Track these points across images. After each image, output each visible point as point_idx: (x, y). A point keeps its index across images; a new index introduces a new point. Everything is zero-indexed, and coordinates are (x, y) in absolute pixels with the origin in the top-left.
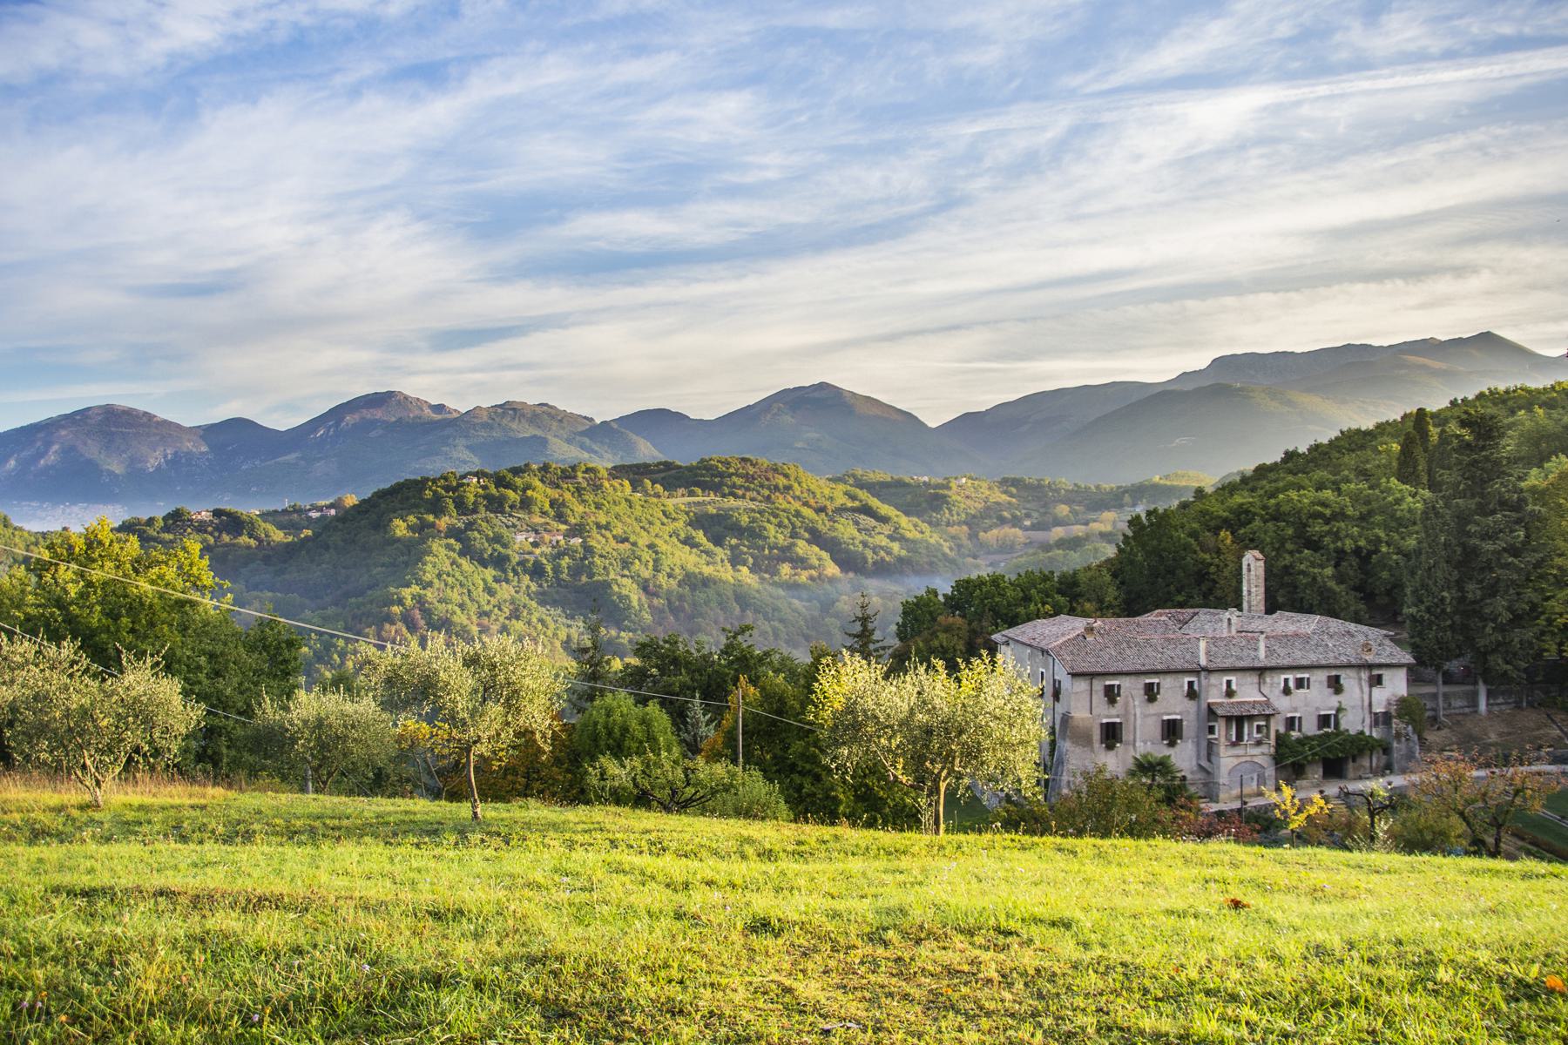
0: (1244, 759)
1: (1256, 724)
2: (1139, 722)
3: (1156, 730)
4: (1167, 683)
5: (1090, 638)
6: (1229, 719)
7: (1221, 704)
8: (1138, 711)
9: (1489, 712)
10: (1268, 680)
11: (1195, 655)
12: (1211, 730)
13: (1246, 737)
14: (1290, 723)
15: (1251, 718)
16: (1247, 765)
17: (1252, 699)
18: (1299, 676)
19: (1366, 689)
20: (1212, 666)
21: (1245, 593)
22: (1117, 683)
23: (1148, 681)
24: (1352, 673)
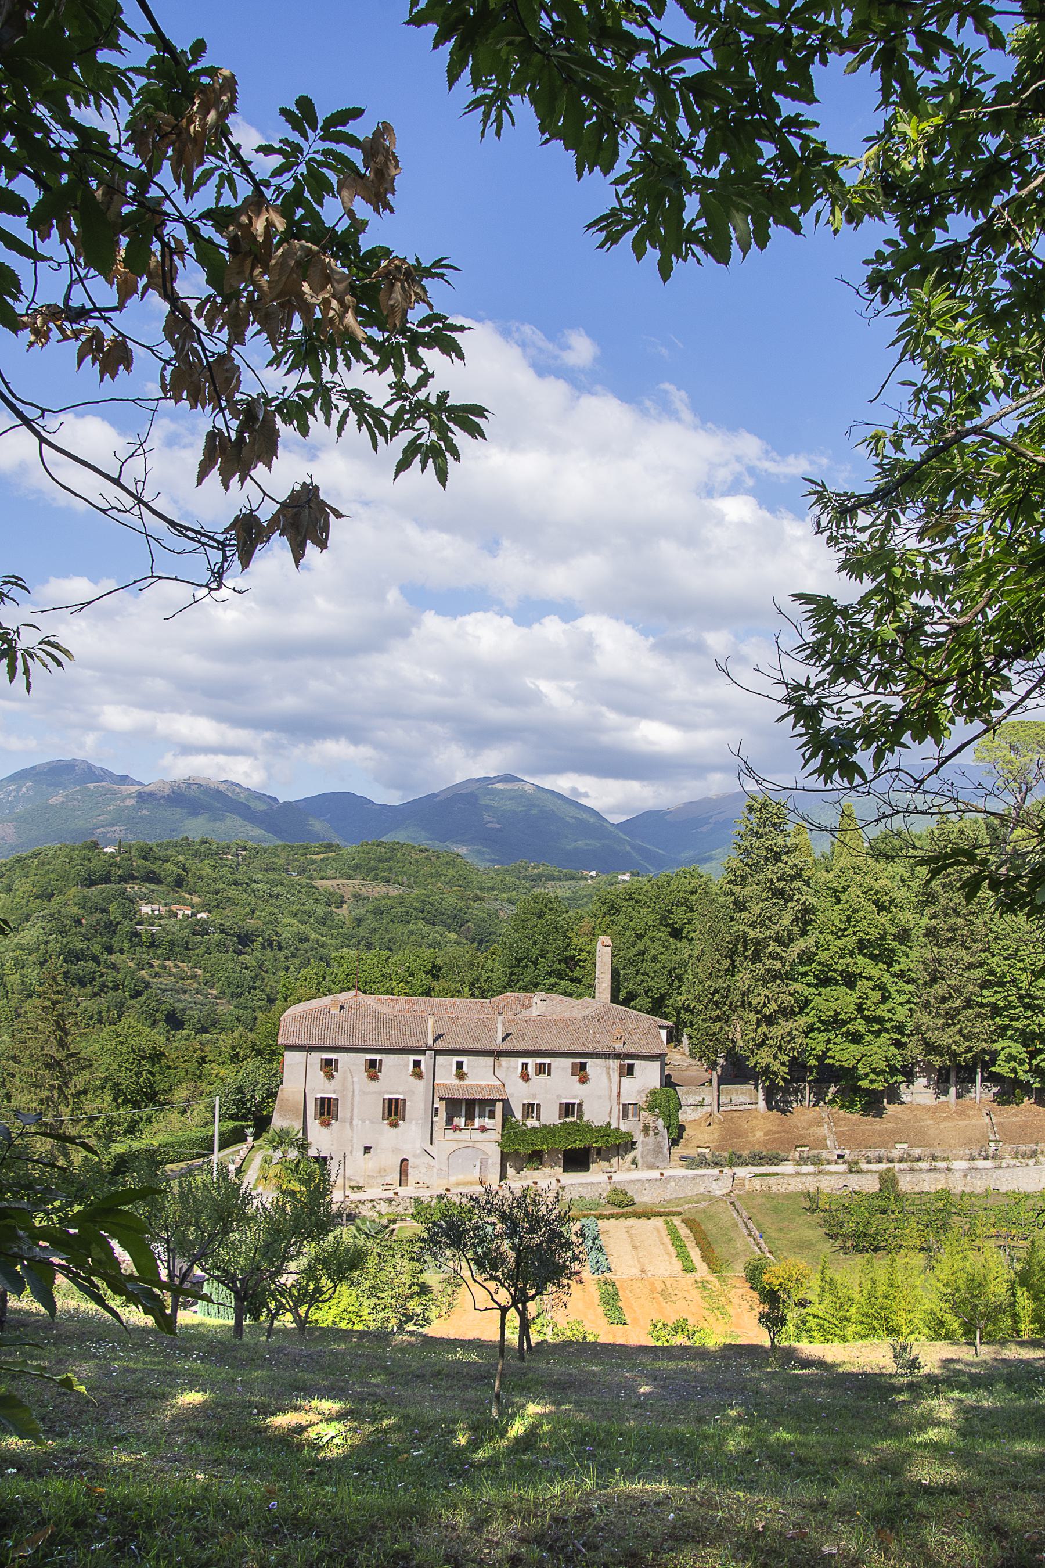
2: (357, 1099)
8: (357, 1087)
16: (470, 1150)
17: (485, 1083)
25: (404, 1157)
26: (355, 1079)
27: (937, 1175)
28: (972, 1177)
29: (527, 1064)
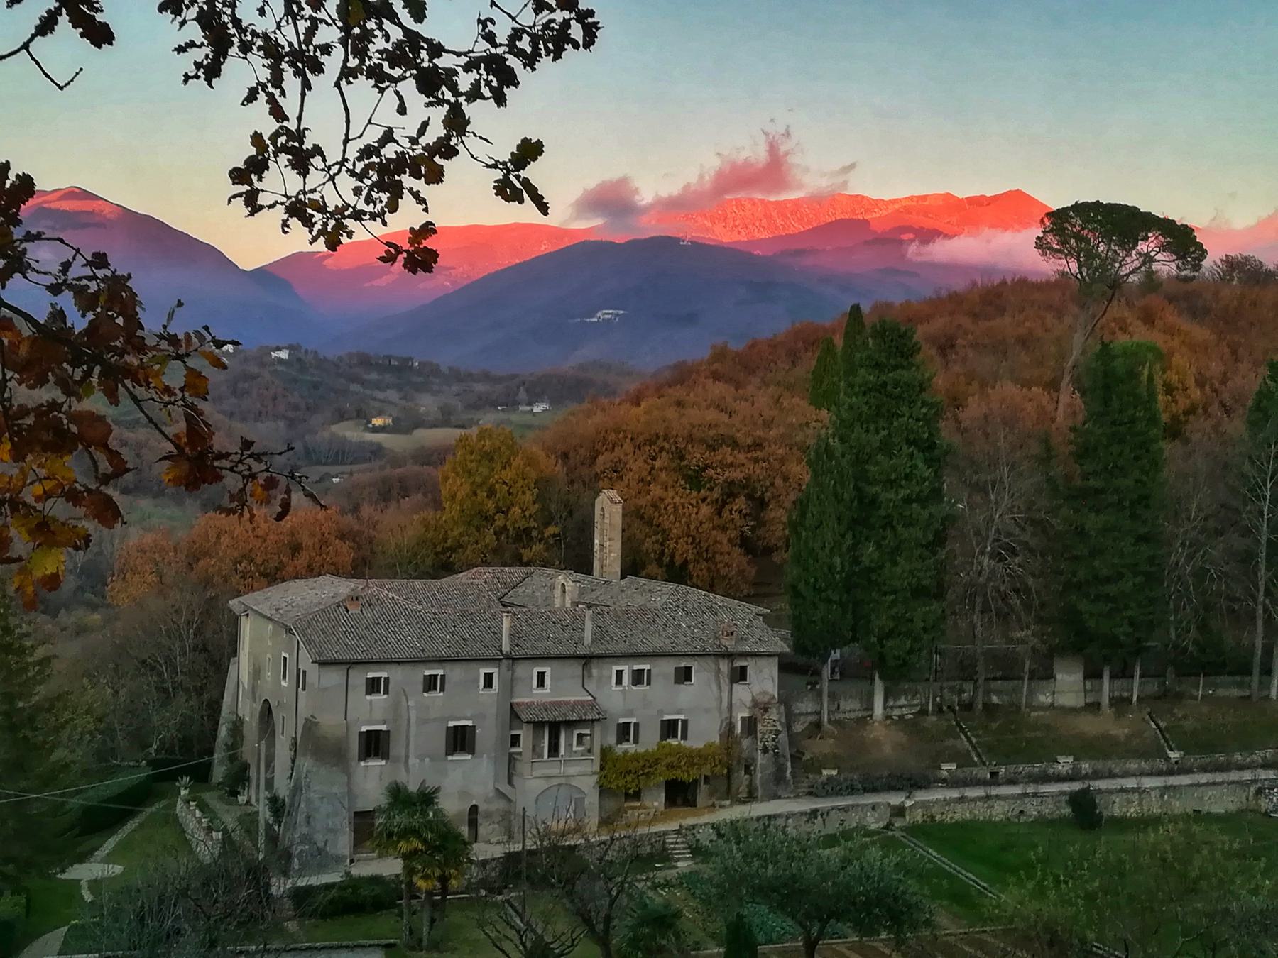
0: (555, 782)
1: (576, 732)
2: (413, 729)
3: (440, 741)
4: (455, 674)
5: (354, 610)
6: (538, 725)
7: (528, 706)
9: (888, 717)
10: (595, 672)
11: (497, 635)
12: (515, 740)
13: (562, 751)
14: (624, 731)
15: (570, 724)
17: (573, 699)
18: (636, 667)
19: (725, 688)
20: (519, 652)
21: (597, 548)
22: (383, 675)
23: (428, 673)
24: (709, 663)
25: (474, 803)
26: (411, 703)
27: (1130, 796)
28: (1169, 797)
29: (622, 671)
